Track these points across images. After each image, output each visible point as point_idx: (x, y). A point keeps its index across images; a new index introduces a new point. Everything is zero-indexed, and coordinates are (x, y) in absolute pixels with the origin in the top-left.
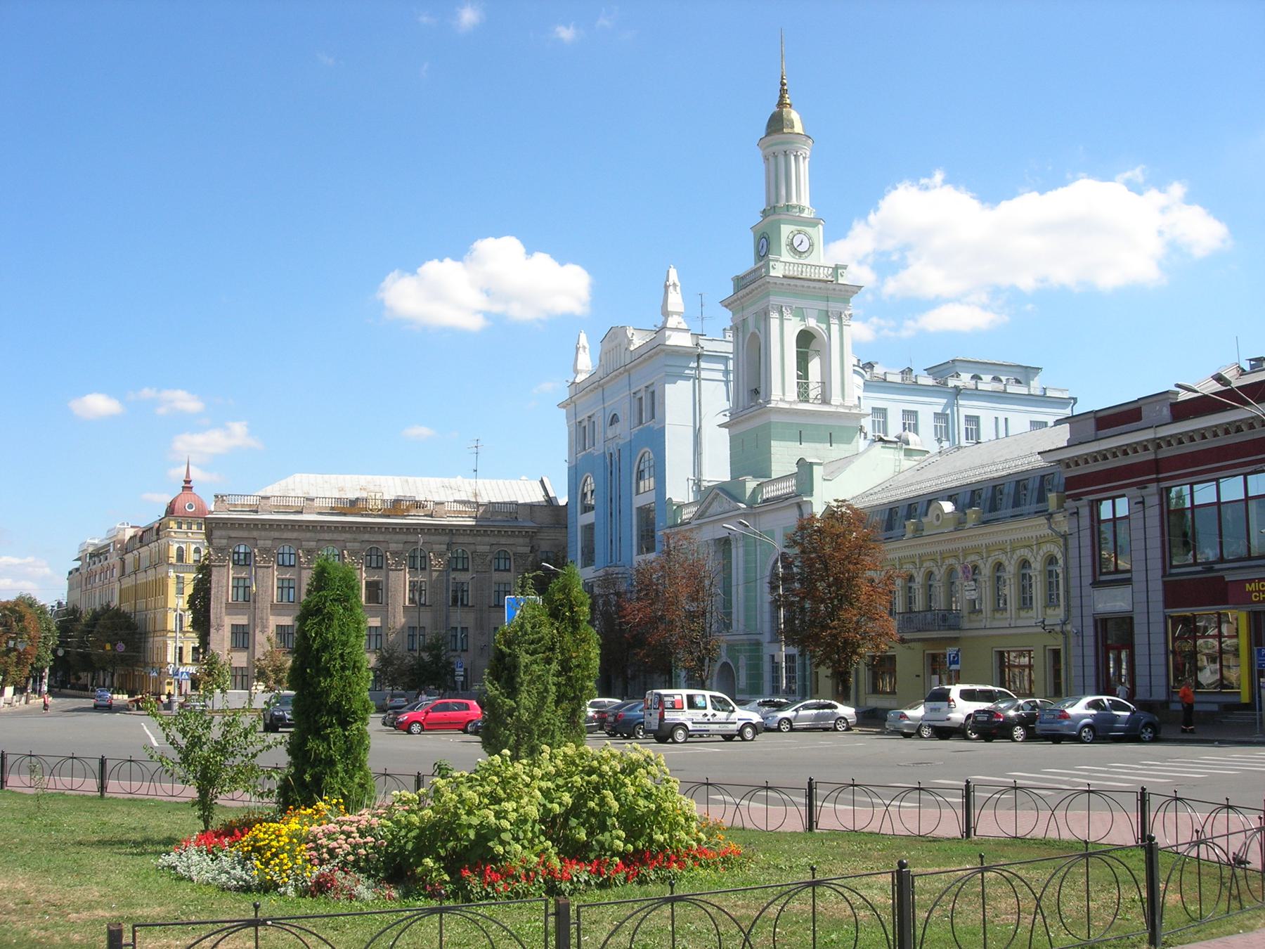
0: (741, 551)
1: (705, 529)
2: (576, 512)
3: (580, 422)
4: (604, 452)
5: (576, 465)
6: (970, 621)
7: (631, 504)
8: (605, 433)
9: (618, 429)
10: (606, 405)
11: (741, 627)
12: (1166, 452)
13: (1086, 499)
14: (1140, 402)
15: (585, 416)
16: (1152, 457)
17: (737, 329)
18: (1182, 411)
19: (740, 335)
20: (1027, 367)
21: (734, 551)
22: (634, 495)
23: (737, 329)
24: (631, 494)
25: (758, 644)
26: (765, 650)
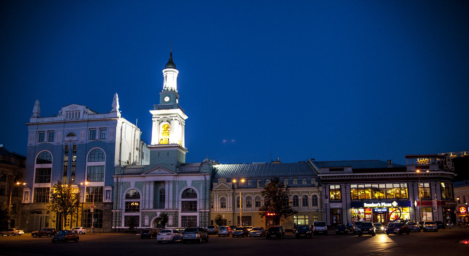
0: (171, 186)
1: (146, 177)
2: (34, 163)
3: (39, 131)
4: (63, 145)
5: (35, 146)
7: (85, 165)
8: (63, 138)
9: (74, 138)
10: (64, 129)
11: (171, 206)
12: (351, 178)
13: (328, 185)
15: (46, 130)
22: (87, 162)
25: (177, 213)
26: (179, 214)
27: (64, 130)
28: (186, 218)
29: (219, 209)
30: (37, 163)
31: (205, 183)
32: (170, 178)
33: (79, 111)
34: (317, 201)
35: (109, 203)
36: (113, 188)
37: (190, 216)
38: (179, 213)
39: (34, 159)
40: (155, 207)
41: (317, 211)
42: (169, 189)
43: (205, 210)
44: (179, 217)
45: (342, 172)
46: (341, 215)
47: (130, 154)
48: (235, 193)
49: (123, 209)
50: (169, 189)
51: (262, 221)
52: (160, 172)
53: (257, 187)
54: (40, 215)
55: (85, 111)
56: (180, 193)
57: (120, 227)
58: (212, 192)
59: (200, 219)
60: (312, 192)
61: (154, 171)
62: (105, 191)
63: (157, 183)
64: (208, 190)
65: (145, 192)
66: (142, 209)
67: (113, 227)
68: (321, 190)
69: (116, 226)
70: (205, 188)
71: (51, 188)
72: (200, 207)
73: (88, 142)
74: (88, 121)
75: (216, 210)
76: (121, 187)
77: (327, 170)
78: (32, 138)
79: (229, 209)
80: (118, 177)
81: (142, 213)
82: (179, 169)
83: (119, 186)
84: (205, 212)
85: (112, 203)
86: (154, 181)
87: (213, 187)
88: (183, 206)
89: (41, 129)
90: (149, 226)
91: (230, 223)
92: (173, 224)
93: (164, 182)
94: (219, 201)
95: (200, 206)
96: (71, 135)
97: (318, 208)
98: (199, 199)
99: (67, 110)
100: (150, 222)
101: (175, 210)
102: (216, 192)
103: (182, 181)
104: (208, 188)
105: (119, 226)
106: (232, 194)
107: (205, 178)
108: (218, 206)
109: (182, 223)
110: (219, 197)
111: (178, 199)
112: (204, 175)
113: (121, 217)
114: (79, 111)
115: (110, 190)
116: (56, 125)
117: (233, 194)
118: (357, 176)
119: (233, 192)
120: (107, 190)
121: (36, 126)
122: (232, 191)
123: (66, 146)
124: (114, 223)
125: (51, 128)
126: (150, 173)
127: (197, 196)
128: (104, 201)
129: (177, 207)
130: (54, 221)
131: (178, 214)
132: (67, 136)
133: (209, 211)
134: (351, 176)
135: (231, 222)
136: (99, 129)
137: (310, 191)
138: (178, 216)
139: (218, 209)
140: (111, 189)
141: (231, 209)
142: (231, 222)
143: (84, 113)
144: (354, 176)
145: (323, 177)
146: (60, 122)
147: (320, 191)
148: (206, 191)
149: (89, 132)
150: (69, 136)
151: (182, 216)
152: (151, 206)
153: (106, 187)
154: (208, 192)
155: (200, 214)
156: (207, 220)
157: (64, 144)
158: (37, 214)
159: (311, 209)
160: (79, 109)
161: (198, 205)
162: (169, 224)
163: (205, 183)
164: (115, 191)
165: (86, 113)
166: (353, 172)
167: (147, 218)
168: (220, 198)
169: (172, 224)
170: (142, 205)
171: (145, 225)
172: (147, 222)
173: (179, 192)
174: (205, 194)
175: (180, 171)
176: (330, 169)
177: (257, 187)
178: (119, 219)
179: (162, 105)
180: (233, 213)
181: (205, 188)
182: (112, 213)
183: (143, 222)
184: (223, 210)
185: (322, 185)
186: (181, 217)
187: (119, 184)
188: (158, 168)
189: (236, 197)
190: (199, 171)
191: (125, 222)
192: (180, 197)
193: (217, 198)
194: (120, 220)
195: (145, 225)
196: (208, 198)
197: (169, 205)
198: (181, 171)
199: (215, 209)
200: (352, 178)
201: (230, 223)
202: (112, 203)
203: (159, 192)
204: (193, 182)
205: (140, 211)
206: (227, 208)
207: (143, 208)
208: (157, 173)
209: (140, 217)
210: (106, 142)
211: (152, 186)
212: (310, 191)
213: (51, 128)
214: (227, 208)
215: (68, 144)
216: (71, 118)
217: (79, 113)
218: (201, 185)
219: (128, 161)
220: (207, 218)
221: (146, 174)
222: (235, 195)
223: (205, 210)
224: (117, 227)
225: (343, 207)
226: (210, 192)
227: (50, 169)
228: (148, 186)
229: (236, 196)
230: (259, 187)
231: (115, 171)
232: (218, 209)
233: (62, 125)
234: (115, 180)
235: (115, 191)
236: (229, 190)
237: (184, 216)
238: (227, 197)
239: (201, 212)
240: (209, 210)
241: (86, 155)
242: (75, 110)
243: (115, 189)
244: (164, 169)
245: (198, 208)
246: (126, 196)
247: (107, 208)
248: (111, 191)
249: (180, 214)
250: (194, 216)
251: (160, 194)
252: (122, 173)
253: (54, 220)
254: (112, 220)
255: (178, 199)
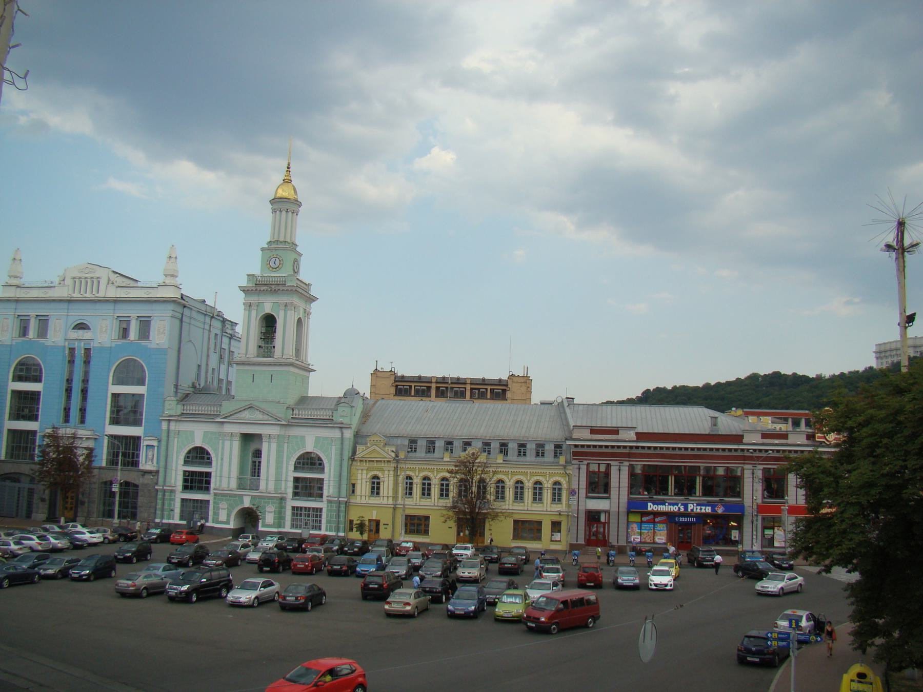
0: (274, 446)
1: (226, 425)
2: (8, 379)
4: (64, 346)
6: (512, 505)
7: (107, 390)
8: (66, 333)
10: (69, 314)
11: (271, 486)
13: (586, 462)
14: (619, 429)
16: (628, 451)
17: (250, 306)
18: (641, 436)
19: (254, 313)
20: (232, 322)
21: (263, 443)
23: (250, 306)
24: (108, 383)
25: (282, 499)
27: (68, 315)
28: (301, 510)
29: (367, 498)
30: (14, 380)
31: (342, 443)
32: (274, 431)
33: (98, 278)
34: (560, 495)
35: (150, 472)
36: (159, 441)
37: (308, 508)
38: (287, 500)
39: (9, 372)
40: (241, 486)
41: (560, 514)
42: (269, 451)
43: (338, 499)
44: (287, 508)
45: (614, 437)
46: (607, 524)
47: (199, 366)
48: (399, 468)
49: (177, 485)
50: (269, 451)
51: (450, 528)
52: (253, 415)
53: (445, 459)
54: (17, 485)
55: (111, 279)
56: (291, 460)
57: (171, 521)
58: (354, 463)
59: (327, 515)
60: (551, 475)
61: (241, 413)
62: (145, 447)
63: (247, 438)
64: (346, 457)
65: (222, 454)
66: (215, 489)
67: (157, 520)
68: (568, 472)
69: (162, 518)
70: (341, 454)
71: (38, 434)
72: (329, 492)
73: (113, 345)
74: (116, 301)
75: (361, 499)
76: (176, 440)
77: (586, 434)
78: (6, 328)
79: (385, 499)
80: (169, 421)
81: (215, 494)
82: (291, 412)
83: (171, 439)
84: (339, 502)
85: (157, 472)
86: (241, 433)
87: (357, 453)
88: (296, 487)
89: (24, 310)
90: (227, 522)
91: (386, 526)
92: (274, 522)
93: (259, 436)
94: (368, 483)
95: (329, 490)
96: (81, 326)
97: (562, 507)
98: (329, 476)
99: (74, 276)
100: (229, 516)
101: (279, 495)
102: (362, 463)
103: (297, 437)
104: (347, 454)
105: (169, 519)
106: (393, 469)
107: (342, 433)
108: (363, 493)
109: (293, 520)
110: (367, 474)
111: (287, 473)
112: (341, 428)
113: (174, 500)
114: (99, 279)
115: (153, 446)
116: (52, 305)
117: (396, 469)
118: (643, 448)
119: (396, 466)
120: (147, 446)
121: (13, 305)
122: (393, 465)
123: (72, 350)
124: (159, 512)
125: (42, 310)
126: (233, 417)
127: (323, 469)
128: (141, 467)
129: (283, 489)
130: (43, 500)
131: (285, 503)
132: (73, 329)
133: (346, 502)
134: (631, 447)
135: (388, 525)
136: (137, 319)
137: (548, 472)
138: (286, 507)
139: (363, 498)
140: (155, 443)
141: (391, 499)
142: (388, 525)
143: (108, 283)
144: (637, 447)
145: (576, 446)
146: (61, 301)
147: (568, 475)
148: (342, 460)
149: (116, 324)
150: (79, 329)
151: (293, 508)
152: (234, 484)
153: (146, 438)
154: (345, 464)
155: (328, 506)
156: (342, 519)
157: (67, 344)
158: (12, 482)
159: (549, 510)
160: (98, 276)
161: (325, 487)
162: (266, 521)
163: (342, 443)
164: (163, 448)
165: (113, 283)
166: (637, 438)
167: (224, 505)
168: (369, 476)
169: (273, 522)
170: (216, 479)
171: (219, 520)
172: (223, 516)
173: (288, 459)
174: (341, 466)
175: (293, 415)
176: (591, 430)
177: (443, 458)
178: (170, 504)
179: (264, 275)
180: (393, 508)
181: (341, 454)
182: (157, 490)
183: (216, 514)
184: (374, 500)
185: (574, 462)
186: (290, 508)
187: (172, 434)
188: (249, 407)
189: (401, 476)
190: (331, 418)
191: (182, 512)
192: (292, 468)
193: (364, 477)
194: (172, 508)
195: (219, 520)
196: (345, 473)
197: (267, 481)
198: (294, 416)
199: (359, 498)
200: (634, 451)
201: (386, 528)
202: (157, 472)
203: (251, 454)
204: (317, 438)
205: (212, 491)
206: (382, 498)
207: (218, 485)
208: (247, 417)
209: (211, 503)
210: (149, 347)
211: (237, 444)
212: (548, 472)
213: (42, 310)
214: (382, 498)
215: (75, 344)
216: (82, 292)
217: (99, 282)
218: (333, 447)
219: (193, 383)
220: (342, 514)
221: (225, 418)
222: (399, 472)
223: (338, 499)
224: (165, 521)
225: (612, 510)
226: (350, 463)
227: (38, 393)
228: (227, 443)
229: (401, 473)
230: (448, 459)
231: (166, 408)
232: (363, 498)
233: (65, 305)
234: (164, 425)
235: (163, 448)
236: (388, 461)
237: (297, 507)
238: (384, 475)
239: (329, 502)
240: (346, 500)
241: (109, 369)
242: (89, 275)
243: (164, 443)
244: (260, 411)
245: (325, 493)
246: (185, 458)
247: (146, 482)
248: (156, 448)
249: (291, 503)
250: (317, 509)
251: (252, 459)
252: (179, 413)
253: (44, 497)
254: (156, 505)
255: (287, 473)
